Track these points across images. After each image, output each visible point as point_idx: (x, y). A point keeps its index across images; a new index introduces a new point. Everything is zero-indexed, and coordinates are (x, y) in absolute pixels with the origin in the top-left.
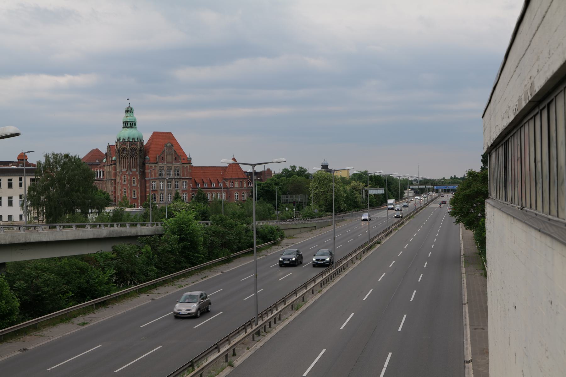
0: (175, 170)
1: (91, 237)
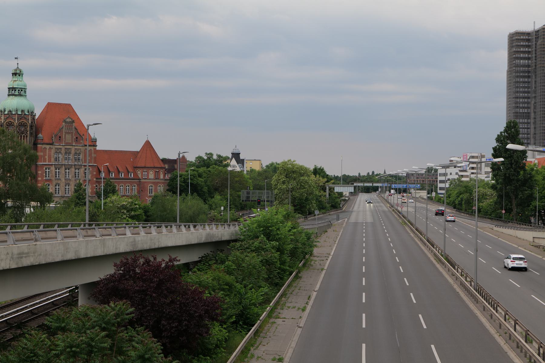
0: (76, 153)
1: (194, 241)
